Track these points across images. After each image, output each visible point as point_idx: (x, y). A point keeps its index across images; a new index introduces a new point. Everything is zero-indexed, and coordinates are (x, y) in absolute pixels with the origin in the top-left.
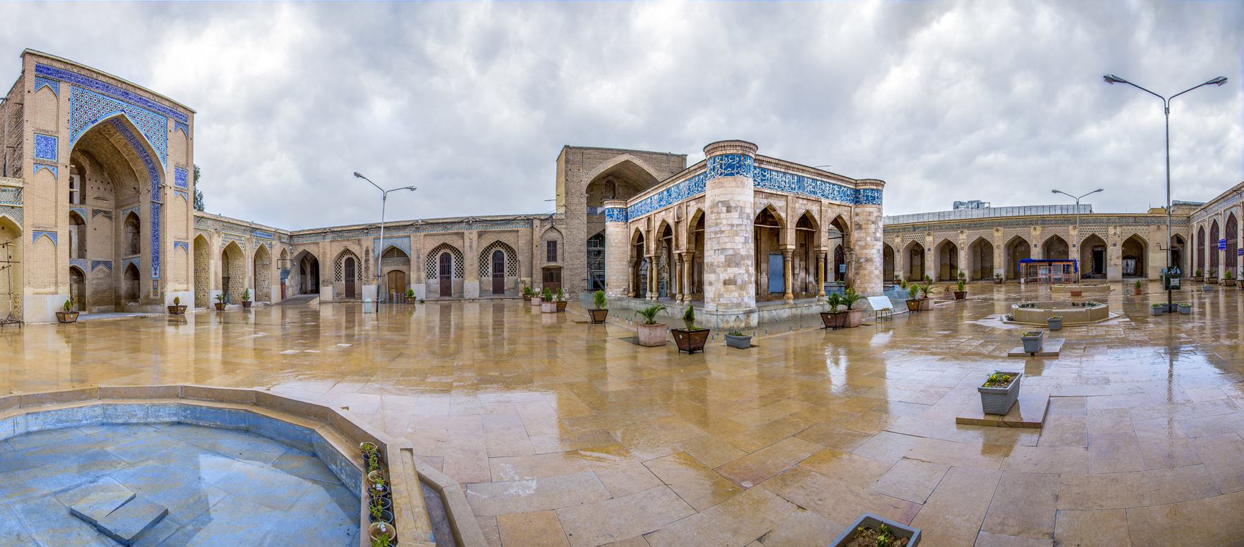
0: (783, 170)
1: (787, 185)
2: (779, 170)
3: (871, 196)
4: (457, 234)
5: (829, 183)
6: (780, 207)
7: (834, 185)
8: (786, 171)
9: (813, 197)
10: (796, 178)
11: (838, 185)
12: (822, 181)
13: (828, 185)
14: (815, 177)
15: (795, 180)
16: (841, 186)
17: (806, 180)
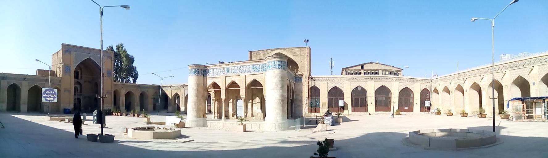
0: (219, 67)
1: (221, 73)
2: (217, 67)
3: (269, 66)
4: (167, 90)
5: (246, 66)
6: (218, 82)
7: (249, 65)
8: (221, 67)
9: (235, 74)
10: (225, 68)
11: (252, 65)
12: (241, 66)
13: (245, 67)
14: (235, 66)
15: (225, 70)
16: (254, 65)
17: (231, 68)
